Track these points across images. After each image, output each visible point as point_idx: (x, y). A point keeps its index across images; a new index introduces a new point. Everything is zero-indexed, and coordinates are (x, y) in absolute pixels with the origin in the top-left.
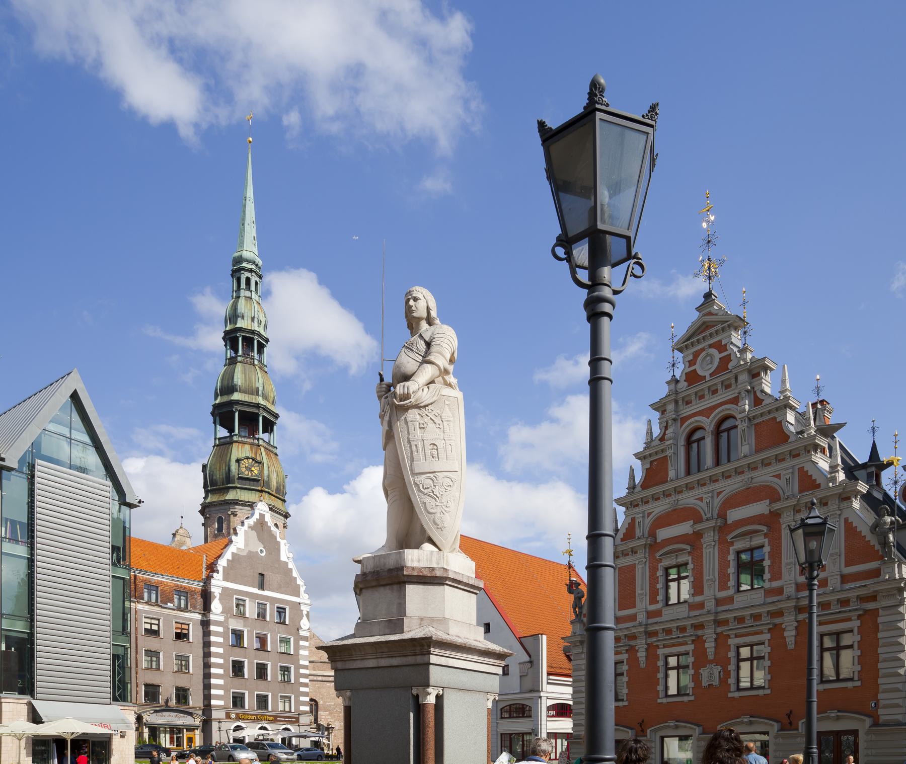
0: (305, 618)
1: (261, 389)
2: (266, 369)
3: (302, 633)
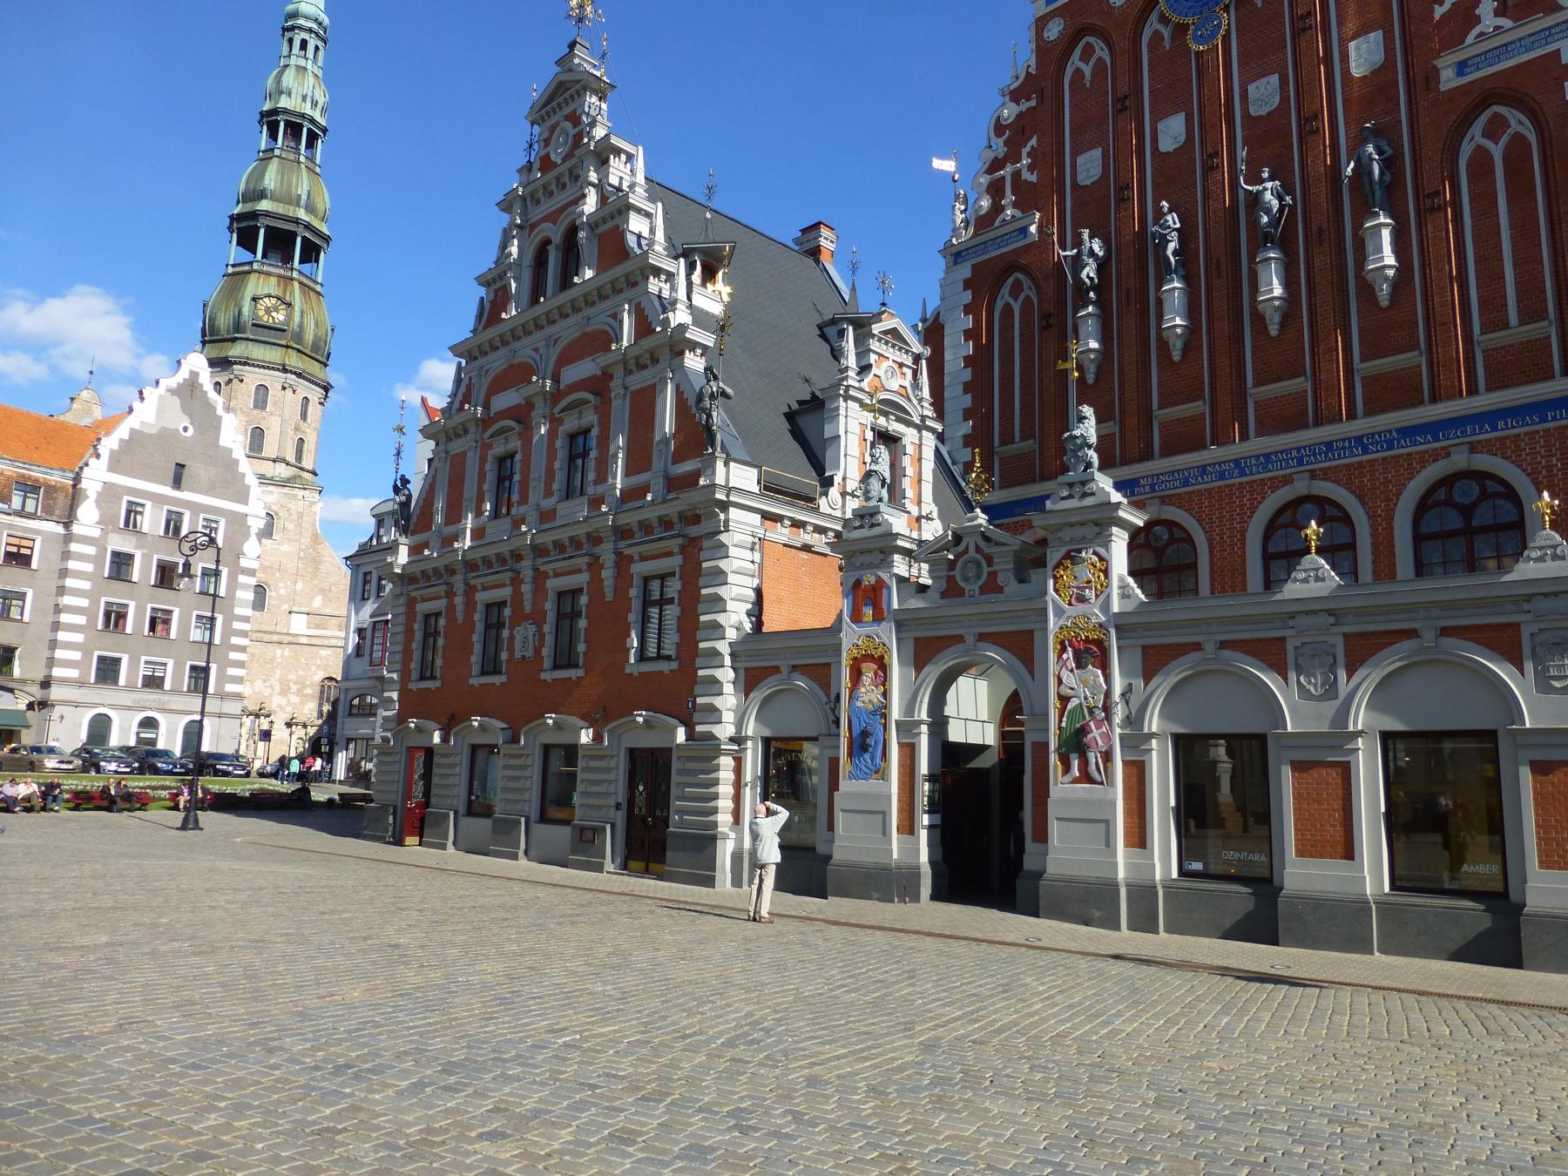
1: (304, 197)
2: (318, 170)
3: (244, 563)
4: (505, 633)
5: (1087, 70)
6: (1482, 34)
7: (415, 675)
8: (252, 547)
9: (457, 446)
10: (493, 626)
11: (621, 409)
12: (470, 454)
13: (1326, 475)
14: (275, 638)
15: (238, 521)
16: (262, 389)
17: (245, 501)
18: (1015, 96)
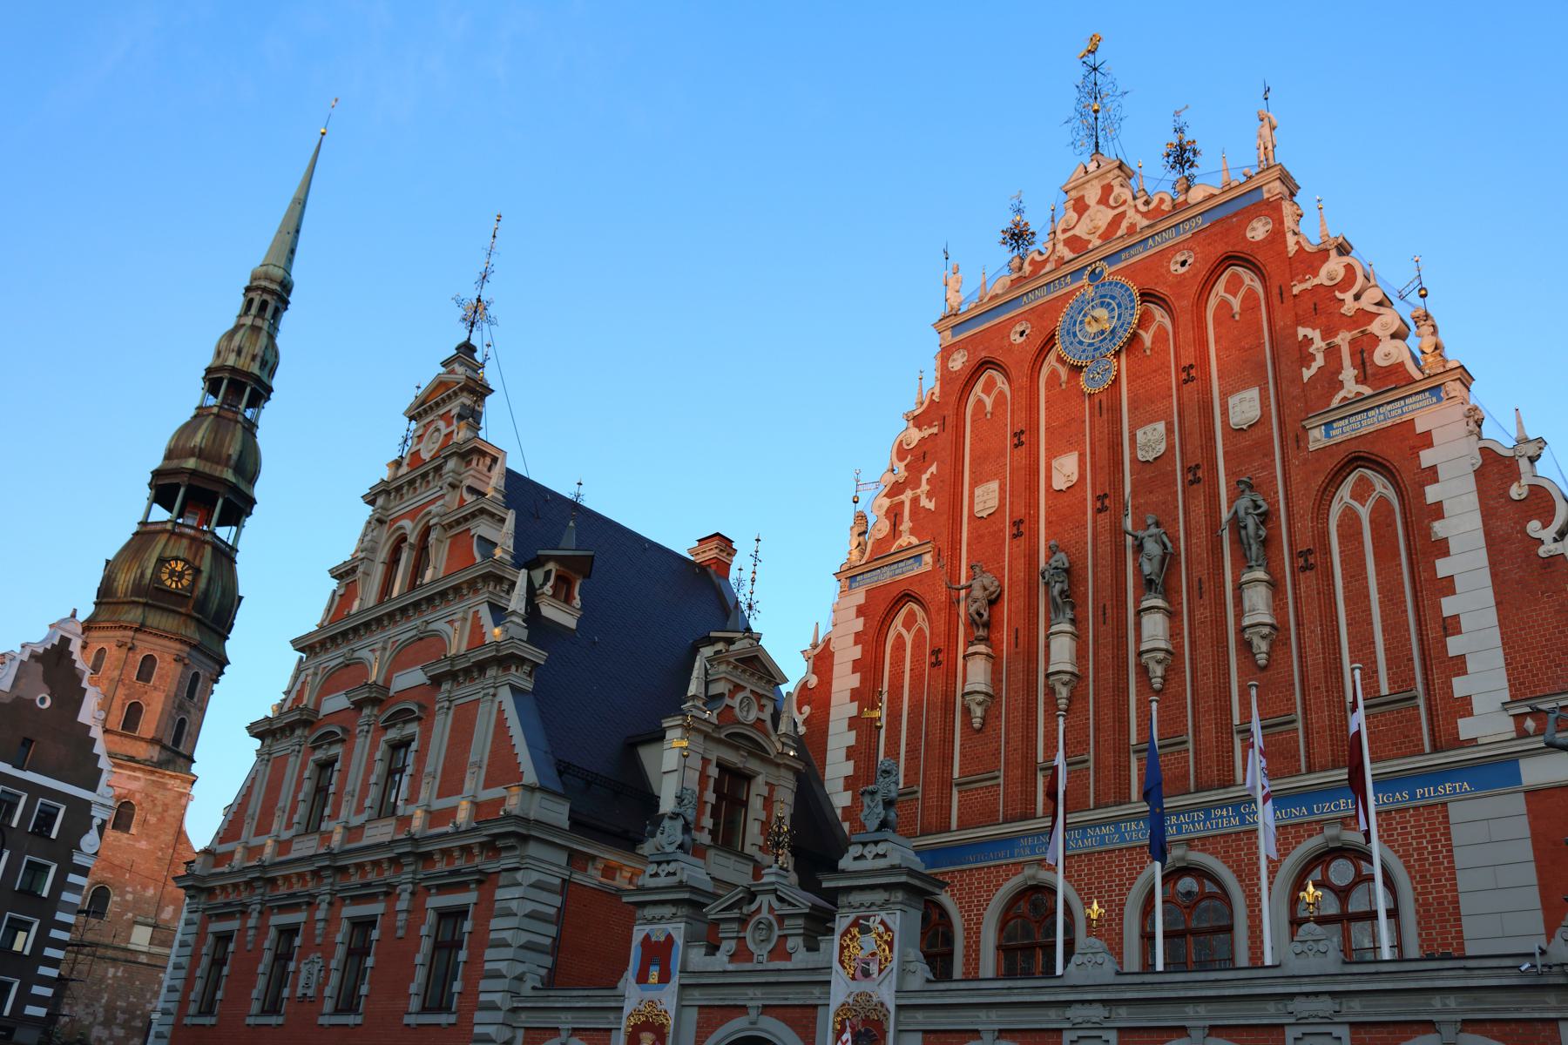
0: (94, 832)
1: (235, 457)
3: (78, 859)
4: (292, 966)
5: (989, 402)
6: (1345, 398)
7: (193, 1008)
8: (90, 841)
9: (282, 746)
10: (282, 957)
11: (442, 727)
12: (292, 759)
13: (1204, 843)
14: (110, 953)
15: (80, 810)
16: (149, 662)
17: (93, 789)
18: (918, 421)
